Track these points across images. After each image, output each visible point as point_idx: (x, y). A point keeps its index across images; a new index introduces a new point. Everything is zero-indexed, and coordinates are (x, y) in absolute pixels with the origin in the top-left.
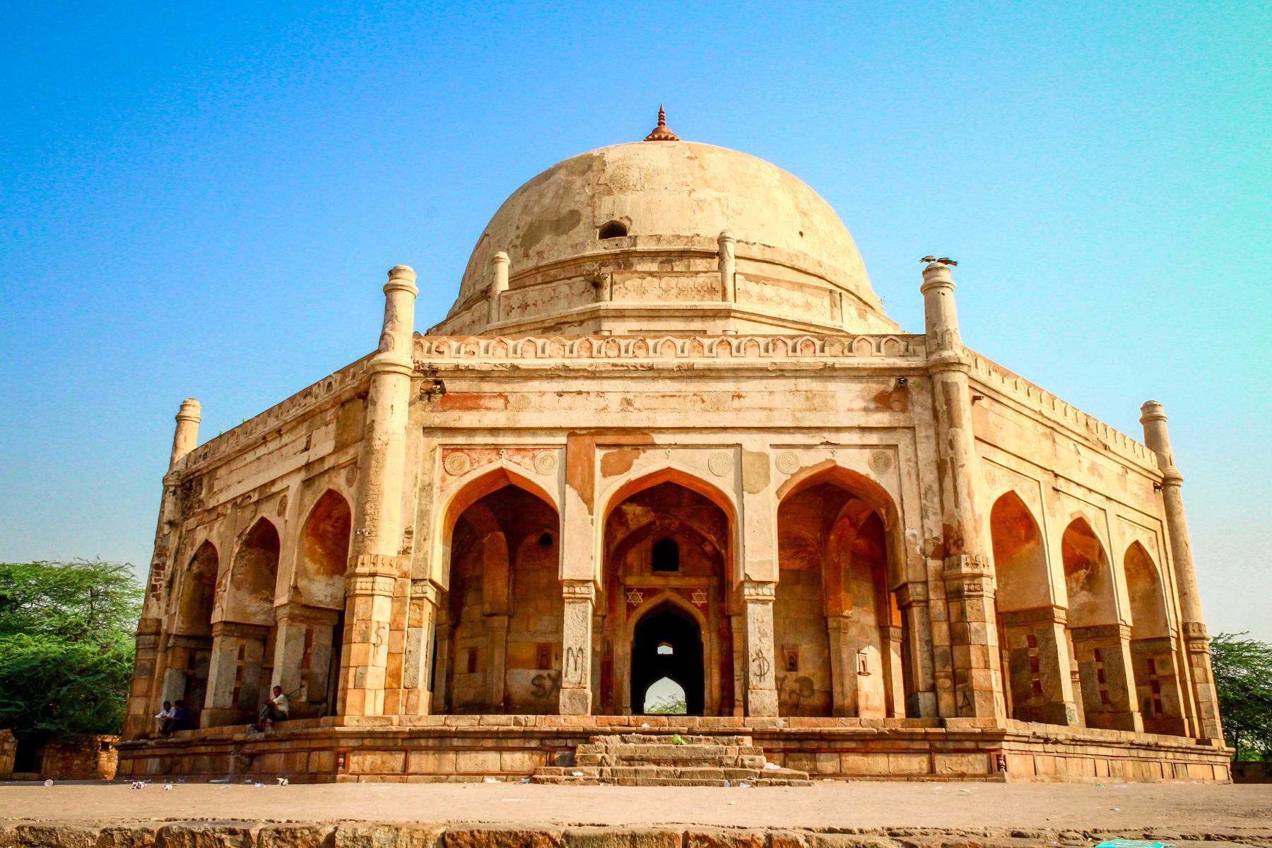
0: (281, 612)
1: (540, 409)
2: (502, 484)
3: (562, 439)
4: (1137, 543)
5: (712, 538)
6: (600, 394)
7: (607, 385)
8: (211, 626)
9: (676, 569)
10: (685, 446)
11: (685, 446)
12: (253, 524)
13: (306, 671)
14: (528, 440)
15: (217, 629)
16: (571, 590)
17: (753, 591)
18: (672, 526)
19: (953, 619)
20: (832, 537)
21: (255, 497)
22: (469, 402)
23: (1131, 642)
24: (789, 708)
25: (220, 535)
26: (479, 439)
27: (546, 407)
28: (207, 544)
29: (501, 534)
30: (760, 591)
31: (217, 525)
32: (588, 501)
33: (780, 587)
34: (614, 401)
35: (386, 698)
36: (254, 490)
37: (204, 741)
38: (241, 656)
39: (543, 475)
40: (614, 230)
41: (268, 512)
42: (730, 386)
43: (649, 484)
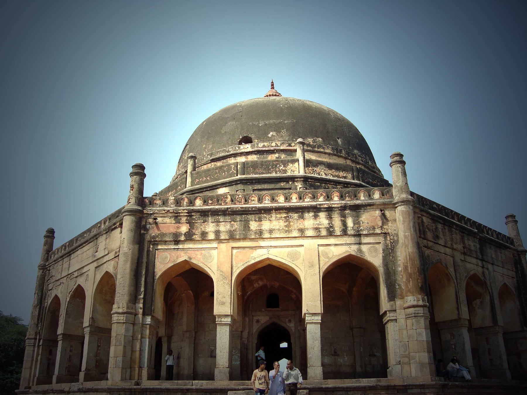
0: (85, 330)
2: (187, 267)
4: (505, 284)
5: (294, 291)
8: (58, 335)
9: (277, 306)
10: (275, 247)
11: (275, 247)
12: (75, 287)
13: (98, 358)
15: (60, 338)
16: (220, 320)
17: (309, 318)
19: (409, 328)
20: (354, 289)
21: (76, 274)
23: (504, 334)
24: (327, 375)
25: (61, 292)
28: (56, 297)
29: (191, 292)
30: (313, 318)
31: (60, 287)
33: (323, 316)
35: (131, 372)
36: (75, 271)
37: (53, 391)
38: (71, 351)
41: (81, 281)
43: (260, 266)
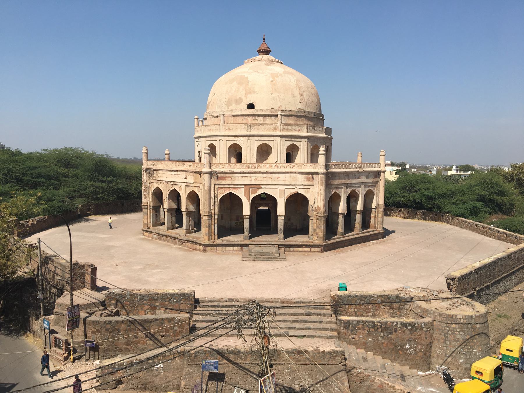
1: (238, 180)
3: (243, 186)
6: (250, 177)
7: (252, 175)
14: (236, 186)
18: (264, 203)
22: (224, 178)
26: (226, 186)
27: (239, 180)
32: (249, 200)
34: (253, 178)
39: (240, 193)
40: (251, 106)
42: (277, 175)
